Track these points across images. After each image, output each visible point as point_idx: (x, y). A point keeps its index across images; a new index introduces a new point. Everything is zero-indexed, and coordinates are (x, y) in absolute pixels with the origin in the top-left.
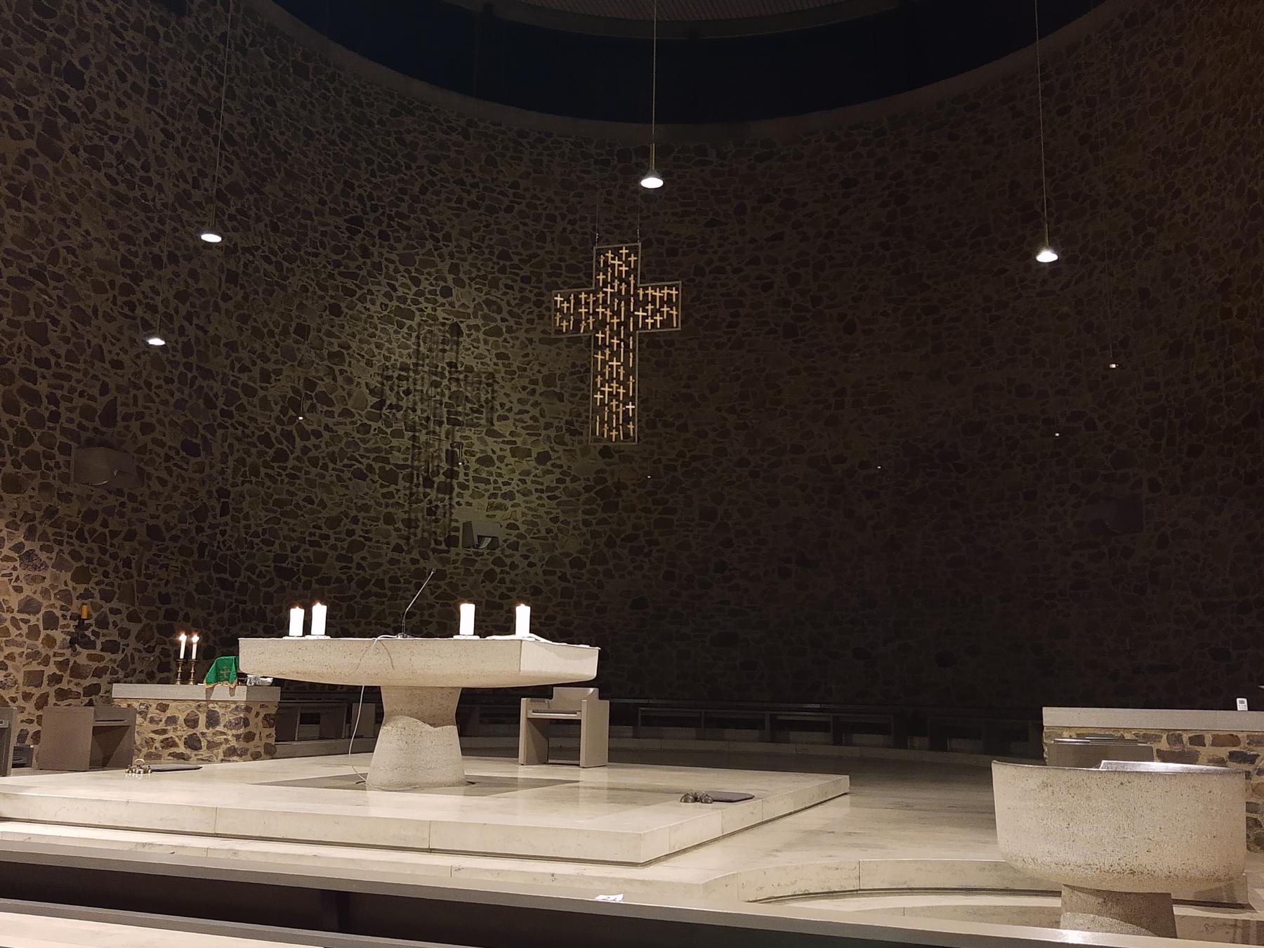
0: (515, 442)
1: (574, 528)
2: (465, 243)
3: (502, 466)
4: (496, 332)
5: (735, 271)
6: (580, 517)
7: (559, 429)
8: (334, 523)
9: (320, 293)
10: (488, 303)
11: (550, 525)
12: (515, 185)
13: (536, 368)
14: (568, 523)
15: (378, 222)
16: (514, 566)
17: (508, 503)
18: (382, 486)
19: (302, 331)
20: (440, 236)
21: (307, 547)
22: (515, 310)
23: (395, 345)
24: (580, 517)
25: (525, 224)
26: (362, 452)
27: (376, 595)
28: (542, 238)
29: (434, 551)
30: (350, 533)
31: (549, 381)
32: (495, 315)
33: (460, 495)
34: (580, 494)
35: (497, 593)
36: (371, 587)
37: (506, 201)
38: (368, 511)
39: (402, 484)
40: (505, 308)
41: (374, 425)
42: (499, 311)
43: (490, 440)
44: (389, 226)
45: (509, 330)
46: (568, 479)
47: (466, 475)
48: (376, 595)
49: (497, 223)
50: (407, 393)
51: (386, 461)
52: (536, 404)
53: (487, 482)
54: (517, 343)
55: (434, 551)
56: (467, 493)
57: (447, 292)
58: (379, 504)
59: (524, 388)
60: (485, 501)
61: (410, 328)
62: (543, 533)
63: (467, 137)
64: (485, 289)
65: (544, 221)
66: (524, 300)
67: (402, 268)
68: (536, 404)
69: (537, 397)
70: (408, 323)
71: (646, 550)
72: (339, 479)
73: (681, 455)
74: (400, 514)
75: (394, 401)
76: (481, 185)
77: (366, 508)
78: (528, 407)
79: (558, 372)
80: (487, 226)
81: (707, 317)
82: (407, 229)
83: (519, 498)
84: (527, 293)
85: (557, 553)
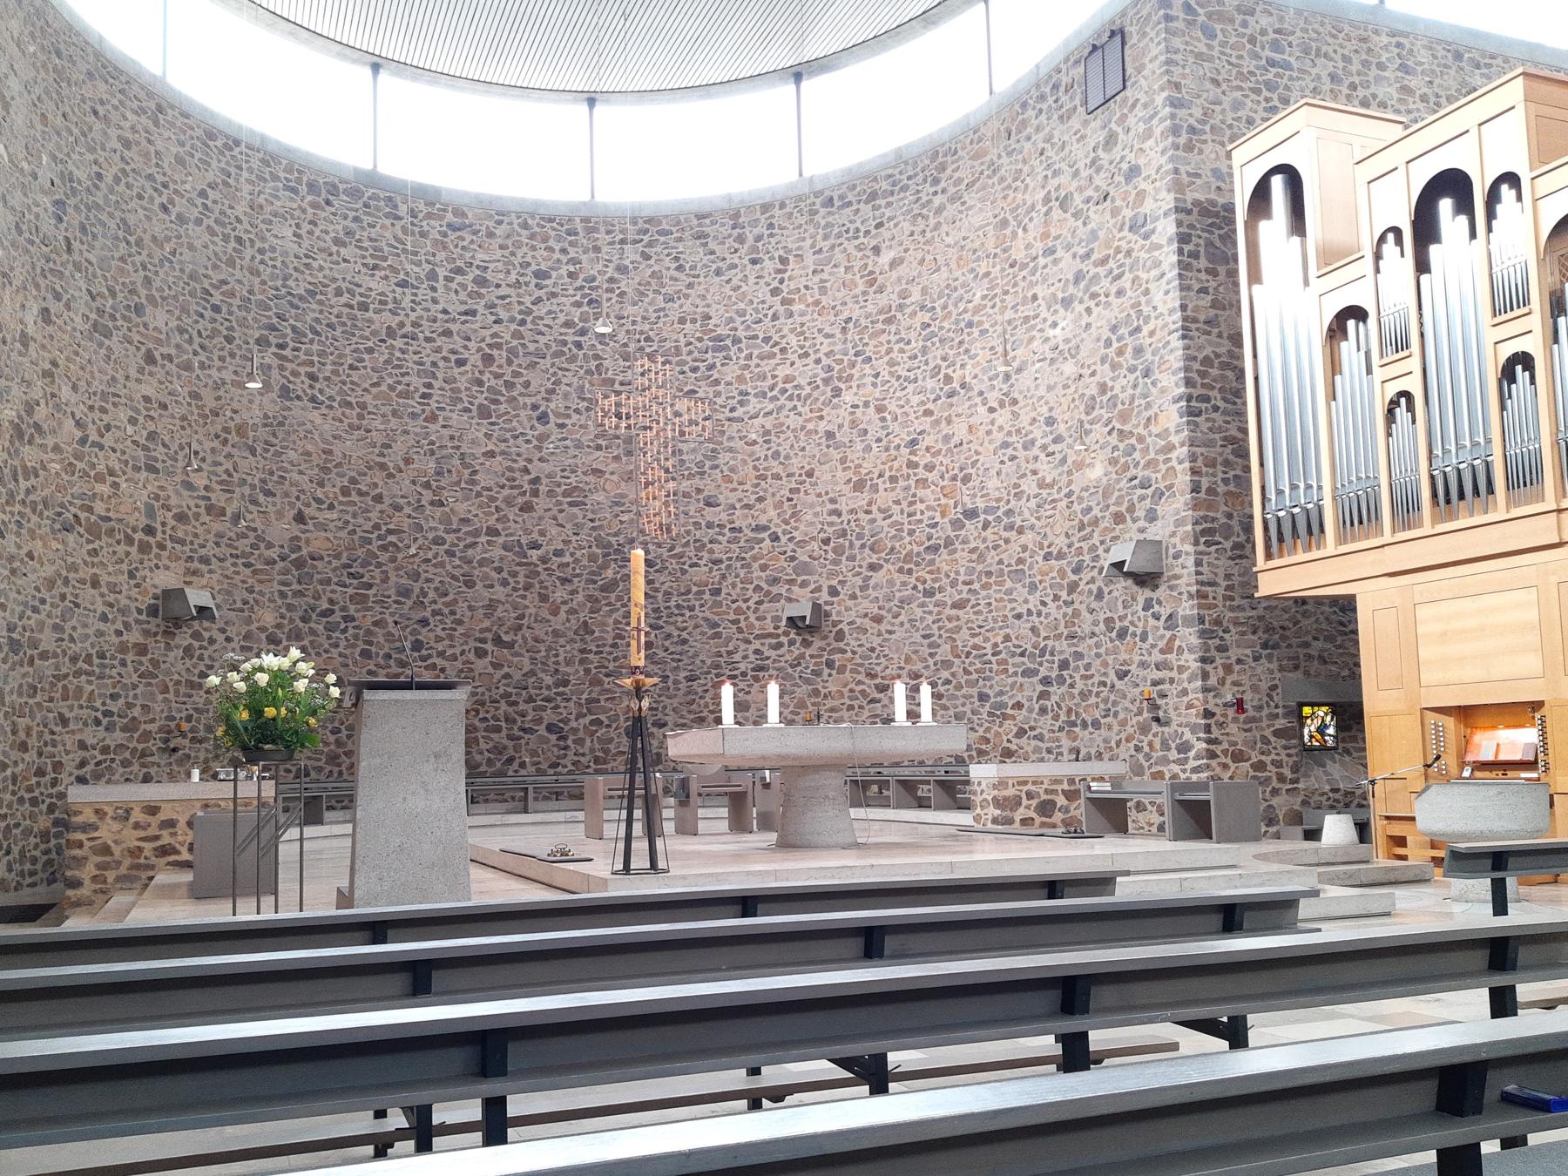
0: (209, 499)
1: (270, 600)
2: (158, 253)
3: (197, 524)
4: (187, 367)
5: (428, 340)
6: (277, 587)
7: (253, 487)
8: (51, 583)
9: (35, 292)
10: (181, 331)
11: (246, 595)
12: (203, 194)
13: (228, 413)
14: (261, 593)
15: (76, 207)
16: (212, 641)
17: (204, 568)
18: (89, 542)
19: (25, 339)
20: (132, 239)
21: (29, 613)
22: (206, 342)
23: (95, 369)
24: (277, 587)
25: (213, 243)
26: (69, 497)
27: (88, 674)
28: (231, 263)
29: (137, 621)
30: (63, 597)
31: (241, 430)
32: (186, 346)
33: (158, 556)
34: (275, 562)
35: (196, 672)
36: (80, 664)
37: (195, 213)
38: (76, 571)
39: (105, 539)
40: (197, 340)
41: (80, 465)
42: (190, 341)
43: (186, 493)
44: (87, 218)
45: (202, 366)
46: (262, 545)
47: (164, 532)
48: (88, 674)
49: (188, 236)
50: (108, 428)
51: (90, 510)
52: (229, 456)
53: (182, 542)
54: (210, 382)
55: (137, 621)
56: (165, 554)
57: (139, 310)
58: (85, 563)
59: (217, 437)
60: (179, 567)
61: (109, 349)
62: (239, 605)
63: (156, 123)
64: (177, 313)
65: (233, 244)
66: (214, 330)
67: (99, 273)
68: (229, 456)
69: (228, 449)
70: (107, 342)
71: (343, 626)
72: (53, 531)
73: (377, 527)
74: (104, 579)
75: (98, 439)
76: (171, 186)
77: (73, 568)
78: (221, 459)
79: (251, 422)
80: (179, 237)
81: (399, 383)
82: (104, 225)
83: (215, 564)
84: (217, 325)
85: (253, 627)
